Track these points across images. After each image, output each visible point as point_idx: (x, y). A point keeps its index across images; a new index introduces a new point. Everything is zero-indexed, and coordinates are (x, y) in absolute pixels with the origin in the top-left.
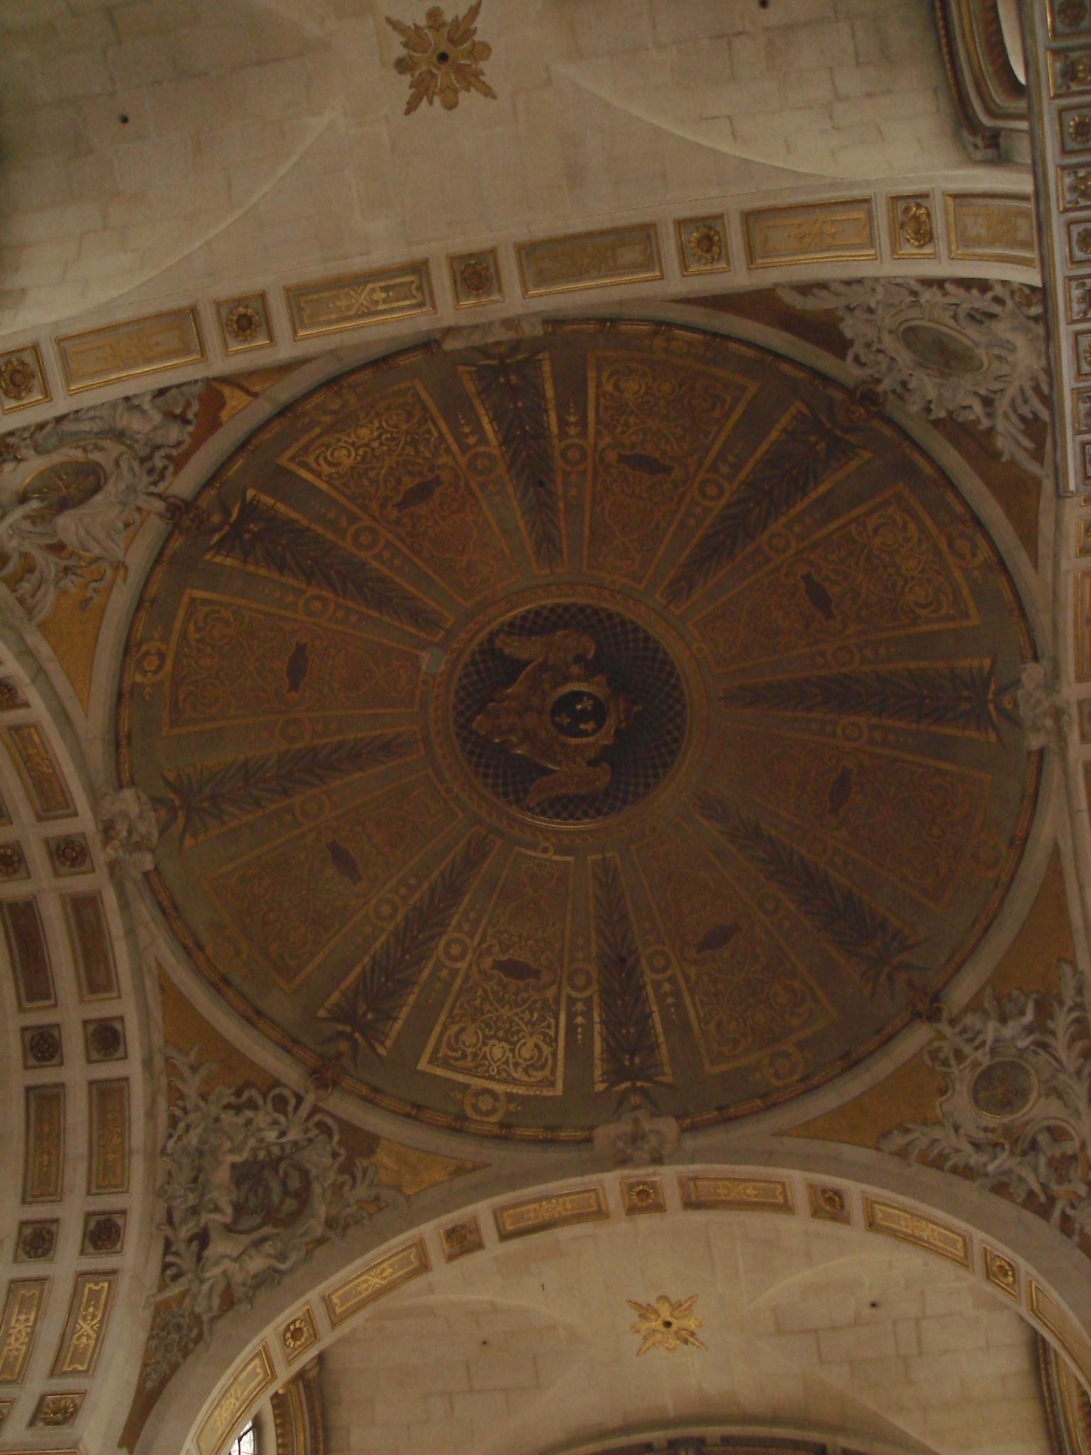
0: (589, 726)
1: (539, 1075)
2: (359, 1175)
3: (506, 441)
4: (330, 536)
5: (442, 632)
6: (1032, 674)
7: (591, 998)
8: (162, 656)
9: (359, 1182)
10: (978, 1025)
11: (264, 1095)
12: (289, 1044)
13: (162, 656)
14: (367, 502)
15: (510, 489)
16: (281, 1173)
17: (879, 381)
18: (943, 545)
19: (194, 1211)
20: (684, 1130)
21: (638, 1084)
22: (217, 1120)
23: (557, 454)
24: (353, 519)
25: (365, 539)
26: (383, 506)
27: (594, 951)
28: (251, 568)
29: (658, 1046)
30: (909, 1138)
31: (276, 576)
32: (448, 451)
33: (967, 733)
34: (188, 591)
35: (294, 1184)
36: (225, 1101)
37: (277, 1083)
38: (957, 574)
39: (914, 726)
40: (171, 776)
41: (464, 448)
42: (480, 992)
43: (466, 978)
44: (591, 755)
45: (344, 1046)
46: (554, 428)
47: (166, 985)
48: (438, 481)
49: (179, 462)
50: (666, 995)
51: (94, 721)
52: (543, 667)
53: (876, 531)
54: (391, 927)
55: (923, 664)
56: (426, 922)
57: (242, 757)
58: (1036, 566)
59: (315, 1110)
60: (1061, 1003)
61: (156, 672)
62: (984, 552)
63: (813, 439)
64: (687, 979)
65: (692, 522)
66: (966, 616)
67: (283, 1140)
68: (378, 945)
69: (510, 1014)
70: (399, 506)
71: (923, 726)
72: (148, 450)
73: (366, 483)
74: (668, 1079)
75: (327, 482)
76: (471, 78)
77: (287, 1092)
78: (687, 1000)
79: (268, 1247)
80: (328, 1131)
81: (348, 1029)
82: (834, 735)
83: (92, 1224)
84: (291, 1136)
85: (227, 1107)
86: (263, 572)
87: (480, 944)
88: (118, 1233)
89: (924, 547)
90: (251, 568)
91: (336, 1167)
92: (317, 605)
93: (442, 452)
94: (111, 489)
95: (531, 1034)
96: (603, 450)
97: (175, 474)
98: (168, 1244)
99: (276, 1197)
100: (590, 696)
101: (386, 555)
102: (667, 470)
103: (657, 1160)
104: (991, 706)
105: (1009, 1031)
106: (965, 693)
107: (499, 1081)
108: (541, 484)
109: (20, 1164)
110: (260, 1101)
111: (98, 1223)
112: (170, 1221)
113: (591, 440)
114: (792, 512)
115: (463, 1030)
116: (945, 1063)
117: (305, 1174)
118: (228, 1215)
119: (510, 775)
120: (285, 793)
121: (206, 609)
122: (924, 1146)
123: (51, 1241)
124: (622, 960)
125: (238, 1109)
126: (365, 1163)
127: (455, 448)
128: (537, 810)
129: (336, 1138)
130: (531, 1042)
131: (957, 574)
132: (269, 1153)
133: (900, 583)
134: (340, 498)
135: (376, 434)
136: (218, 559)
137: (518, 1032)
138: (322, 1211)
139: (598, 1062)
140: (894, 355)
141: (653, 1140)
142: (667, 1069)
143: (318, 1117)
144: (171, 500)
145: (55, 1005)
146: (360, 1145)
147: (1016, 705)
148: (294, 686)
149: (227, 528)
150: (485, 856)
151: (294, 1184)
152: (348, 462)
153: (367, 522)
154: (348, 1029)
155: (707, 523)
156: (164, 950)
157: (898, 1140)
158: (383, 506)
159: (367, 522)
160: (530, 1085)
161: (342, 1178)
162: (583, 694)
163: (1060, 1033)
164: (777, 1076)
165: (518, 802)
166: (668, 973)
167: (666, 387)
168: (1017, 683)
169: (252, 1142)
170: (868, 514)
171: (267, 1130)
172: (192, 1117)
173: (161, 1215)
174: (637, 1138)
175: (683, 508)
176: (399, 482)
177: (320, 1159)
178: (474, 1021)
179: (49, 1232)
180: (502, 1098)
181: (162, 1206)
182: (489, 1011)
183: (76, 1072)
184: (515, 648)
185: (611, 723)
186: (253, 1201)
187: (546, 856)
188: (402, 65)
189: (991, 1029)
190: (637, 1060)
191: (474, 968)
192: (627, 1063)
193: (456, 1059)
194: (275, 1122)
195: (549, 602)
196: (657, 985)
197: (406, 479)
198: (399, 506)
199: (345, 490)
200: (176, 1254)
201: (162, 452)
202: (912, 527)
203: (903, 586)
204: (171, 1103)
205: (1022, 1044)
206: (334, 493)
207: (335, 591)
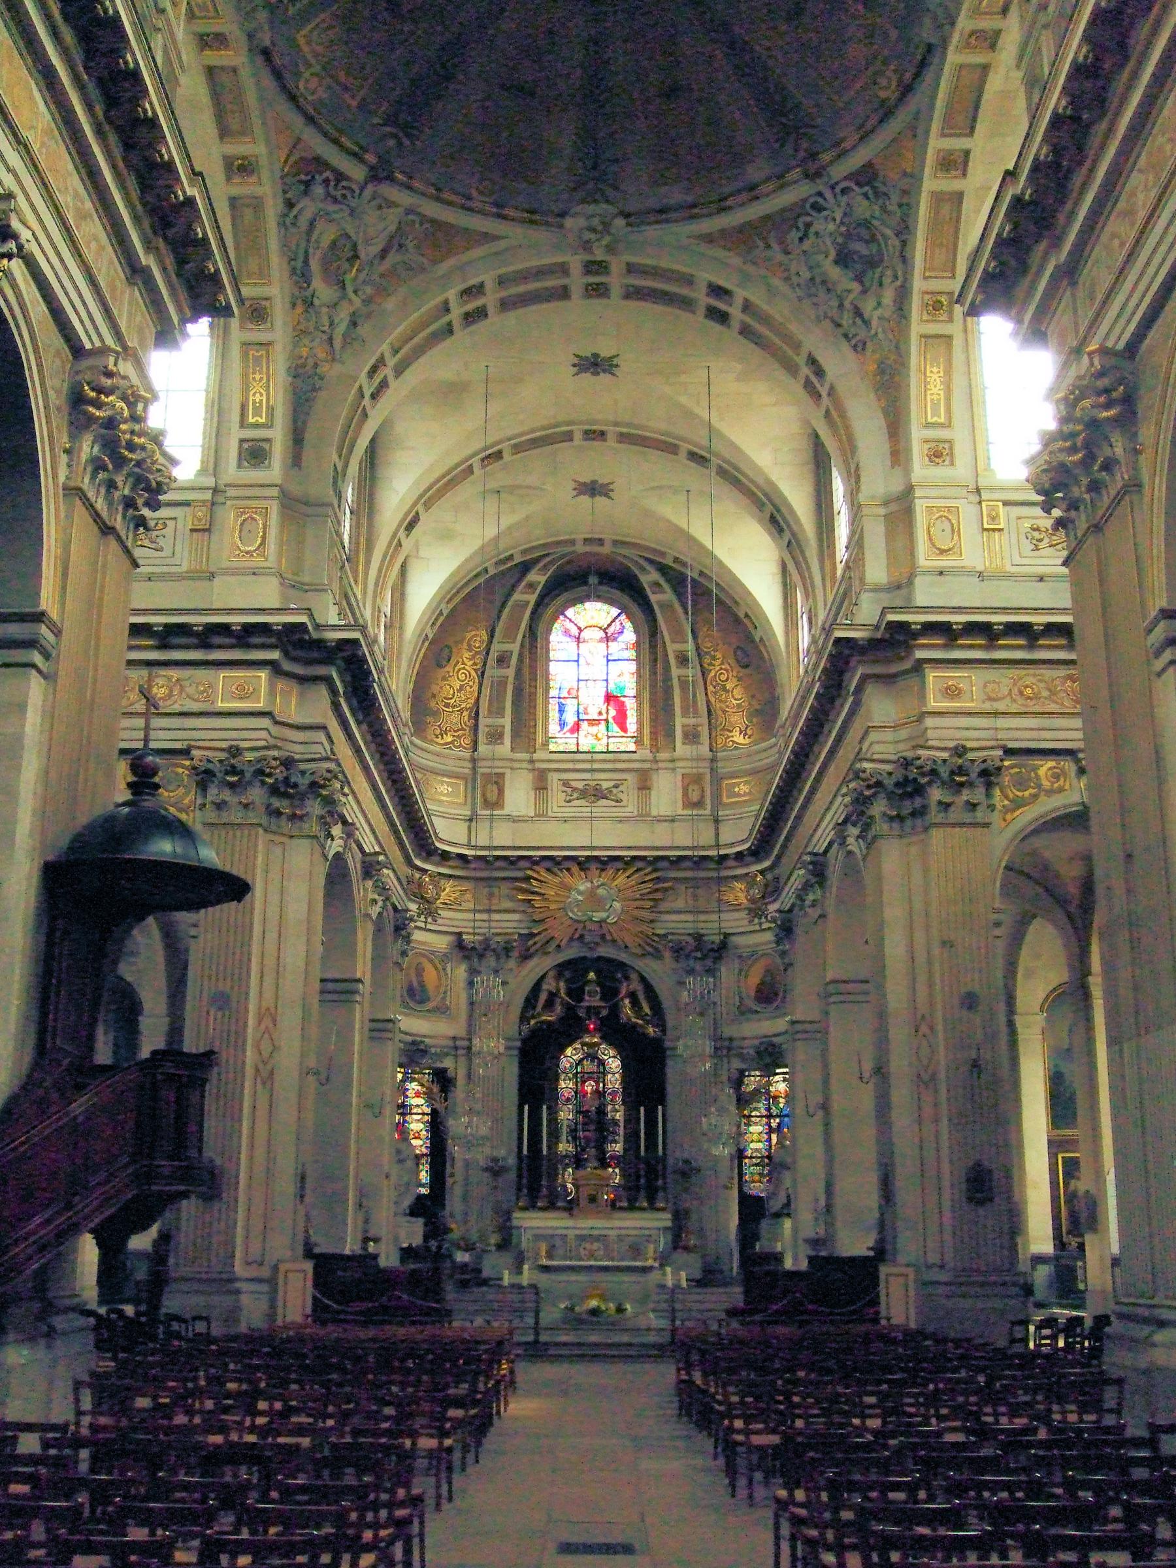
12: (780, 179)
19: (841, 306)
37: (804, 201)
47: (709, 239)
49: (340, 176)
51: (514, 233)
59: (833, 188)
77: (812, 200)
79: (887, 281)
84: (838, 215)
85: (801, 240)
98: (846, 336)
118: (855, 286)
138: (889, 232)
146: (867, 176)
156: (685, 230)
169: (828, 242)
181: (827, 324)
194: (826, 218)
200: (855, 335)
201: (333, 192)
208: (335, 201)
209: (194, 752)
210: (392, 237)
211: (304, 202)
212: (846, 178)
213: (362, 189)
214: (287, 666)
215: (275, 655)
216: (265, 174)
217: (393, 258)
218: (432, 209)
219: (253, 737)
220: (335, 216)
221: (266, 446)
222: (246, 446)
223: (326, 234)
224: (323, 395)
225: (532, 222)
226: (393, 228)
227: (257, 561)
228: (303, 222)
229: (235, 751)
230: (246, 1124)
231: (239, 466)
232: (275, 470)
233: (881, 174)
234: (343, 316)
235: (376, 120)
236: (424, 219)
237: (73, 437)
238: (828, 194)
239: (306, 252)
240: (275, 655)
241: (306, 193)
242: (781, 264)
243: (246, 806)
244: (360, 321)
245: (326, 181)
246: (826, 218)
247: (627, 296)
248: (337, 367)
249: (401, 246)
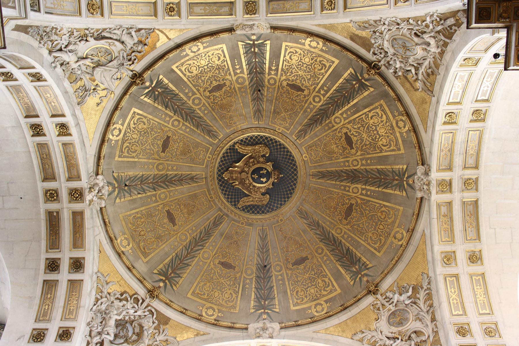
0: (264, 180)
1: (231, 304)
2: (161, 331)
3: (250, 73)
4: (185, 99)
5: (218, 140)
6: (420, 169)
7: (252, 279)
8: (120, 131)
9: (161, 333)
10: (391, 296)
11: (131, 297)
13: (120, 131)
14: (199, 88)
15: (249, 91)
16: (133, 325)
17: (380, 61)
18: (394, 124)
19: (99, 333)
20: (281, 328)
21: (266, 311)
22: (112, 302)
23: (266, 81)
24: (194, 94)
25: (197, 101)
26: (204, 91)
27: (255, 262)
28: (156, 105)
29: (275, 298)
30: (364, 335)
31: (164, 109)
32: (230, 74)
33: (395, 192)
34: (133, 108)
35: (137, 330)
36: (116, 296)
37: (136, 293)
38: (398, 135)
39: (377, 189)
40: (115, 175)
41: (236, 74)
42: (213, 272)
43: (209, 265)
44: (263, 191)
45: (162, 284)
46: (267, 71)
48: (224, 85)
50: (279, 280)
52: (251, 157)
53: (371, 118)
54: (185, 244)
55: (382, 167)
56: (198, 242)
57: (141, 173)
58: (426, 132)
60: (422, 288)
61: (117, 136)
62: (408, 126)
63: (354, 83)
64: (287, 274)
65: (309, 110)
66: (399, 149)
67: (136, 314)
68: (179, 249)
69: (223, 281)
70: (210, 92)
71: (380, 189)
72: (130, 52)
73: (201, 81)
74: (277, 310)
75: (187, 79)
77: (139, 298)
78: (287, 283)
80: (152, 314)
81: (164, 279)
82: (348, 191)
83: (61, 332)
84: (139, 313)
85: (117, 299)
86: (160, 107)
87: (215, 255)
88: (70, 335)
89: (388, 124)
90: (156, 105)
91: (153, 327)
92: (176, 123)
93: (228, 74)
94: (115, 63)
95: (229, 289)
96: (282, 81)
97: (137, 63)
99: (130, 334)
100: (266, 169)
101: (203, 108)
102: (303, 91)
103: (271, 337)
104: (405, 183)
105: (402, 298)
106: (397, 178)
107: (216, 305)
108: (259, 91)
109: (37, 307)
110: (129, 299)
111: (63, 331)
112: (90, 335)
113: (279, 77)
114: (344, 109)
115: (205, 284)
116: (379, 309)
117: (141, 327)
118: (112, 338)
119: (233, 194)
120: (154, 189)
121: (138, 117)
122: (369, 338)
123: (44, 336)
124: (265, 266)
125: (121, 300)
126: (165, 327)
127: (232, 73)
128: (241, 209)
129: (155, 316)
130: (229, 292)
131: (398, 135)
132: (130, 318)
133: (378, 137)
134: (191, 85)
135: (207, 63)
136: (146, 99)
137: (224, 288)
139: (252, 302)
140: (387, 50)
141: (270, 330)
142: (277, 307)
143: (149, 308)
144: (134, 72)
145: (60, 251)
146: (163, 321)
147: (414, 182)
148: (163, 151)
149: (151, 88)
150: (221, 223)
151: (137, 330)
152: (195, 72)
153: (198, 96)
154: (164, 279)
155: (314, 111)
157: (360, 336)
158: (204, 91)
159: (198, 96)
160: (227, 307)
161: (155, 331)
162: (263, 168)
163: (421, 298)
164: (317, 311)
165: (235, 205)
166: (281, 272)
167: (307, 60)
168: (415, 174)
169: (124, 313)
170: (370, 111)
171: (130, 310)
172: (104, 300)
173: (88, 333)
174: (264, 329)
175: (306, 105)
176: (211, 83)
177: (148, 324)
178: (209, 282)
179: (43, 333)
180: (216, 310)
181: (88, 329)
182: (215, 279)
183: (64, 275)
184: (241, 149)
185: (271, 180)
186: (121, 334)
187: (242, 226)
189: (396, 297)
190: (266, 303)
191: (212, 263)
192: (263, 303)
193: (201, 295)
195: (256, 134)
196: (277, 276)
197: (214, 82)
198: (210, 92)
199: (192, 82)
201: (133, 54)
202: (384, 116)
203: (379, 138)
204: (97, 293)
205: (407, 302)
206: (188, 83)
207: (183, 119)
212: (156, 310)
228: (125, 38)
233: (168, 326)
238: (145, 304)
239: (111, 38)
242: (102, 292)
244: (64, 67)
246: (133, 307)
247: (50, 214)
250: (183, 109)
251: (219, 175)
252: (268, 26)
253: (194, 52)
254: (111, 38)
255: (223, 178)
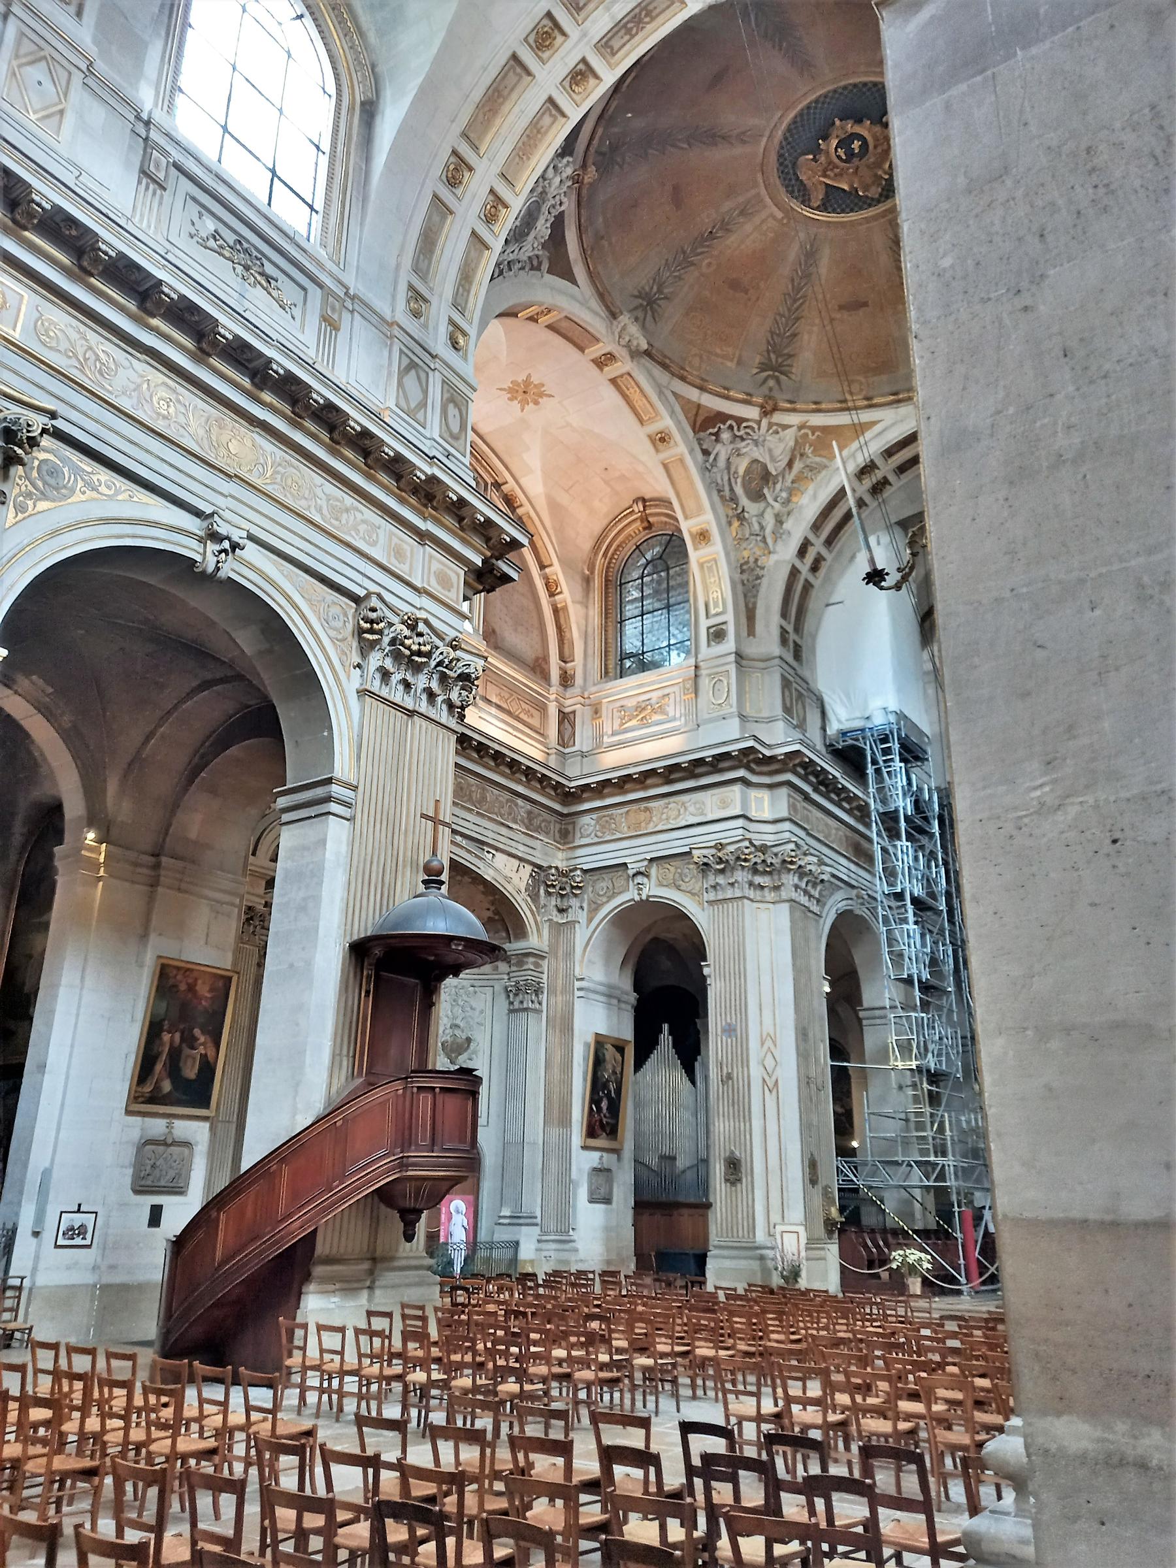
49: (740, 421)
51: (886, 416)
76: (527, 382)
148: (865, 304)
188: (536, 403)
201: (738, 434)
208: (743, 439)
209: (694, 852)
210: (793, 450)
211: (719, 447)
213: (759, 423)
214: (754, 779)
215: (741, 773)
216: (677, 436)
217: (798, 465)
218: (818, 420)
219: (731, 833)
220: (744, 450)
221: (724, 627)
222: (711, 630)
223: (742, 466)
224: (765, 581)
225: (899, 401)
226: (792, 443)
227: (726, 710)
228: (722, 463)
229: (720, 847)
230: (757, 1123)
231: (709, 645)
232: (729, 645)
234: (769, 521)
235: (755, 371)
236: (814, 429)
237: (364, 654)
239: (730, 485)
240: (741, 773)
241: (717, 441)
243: (732, 884)
245: (731, 427)
248: (773, 558)
249: (802, 455)
250: (789, 310)
251: (879, 202)
252: (615, 323)
253: (701, 357)
254: (730, 485)
255: (881, 195)
